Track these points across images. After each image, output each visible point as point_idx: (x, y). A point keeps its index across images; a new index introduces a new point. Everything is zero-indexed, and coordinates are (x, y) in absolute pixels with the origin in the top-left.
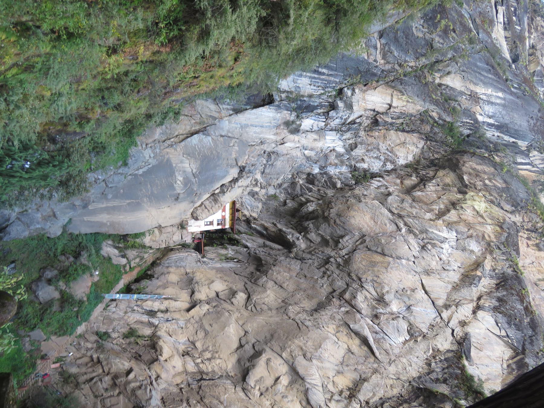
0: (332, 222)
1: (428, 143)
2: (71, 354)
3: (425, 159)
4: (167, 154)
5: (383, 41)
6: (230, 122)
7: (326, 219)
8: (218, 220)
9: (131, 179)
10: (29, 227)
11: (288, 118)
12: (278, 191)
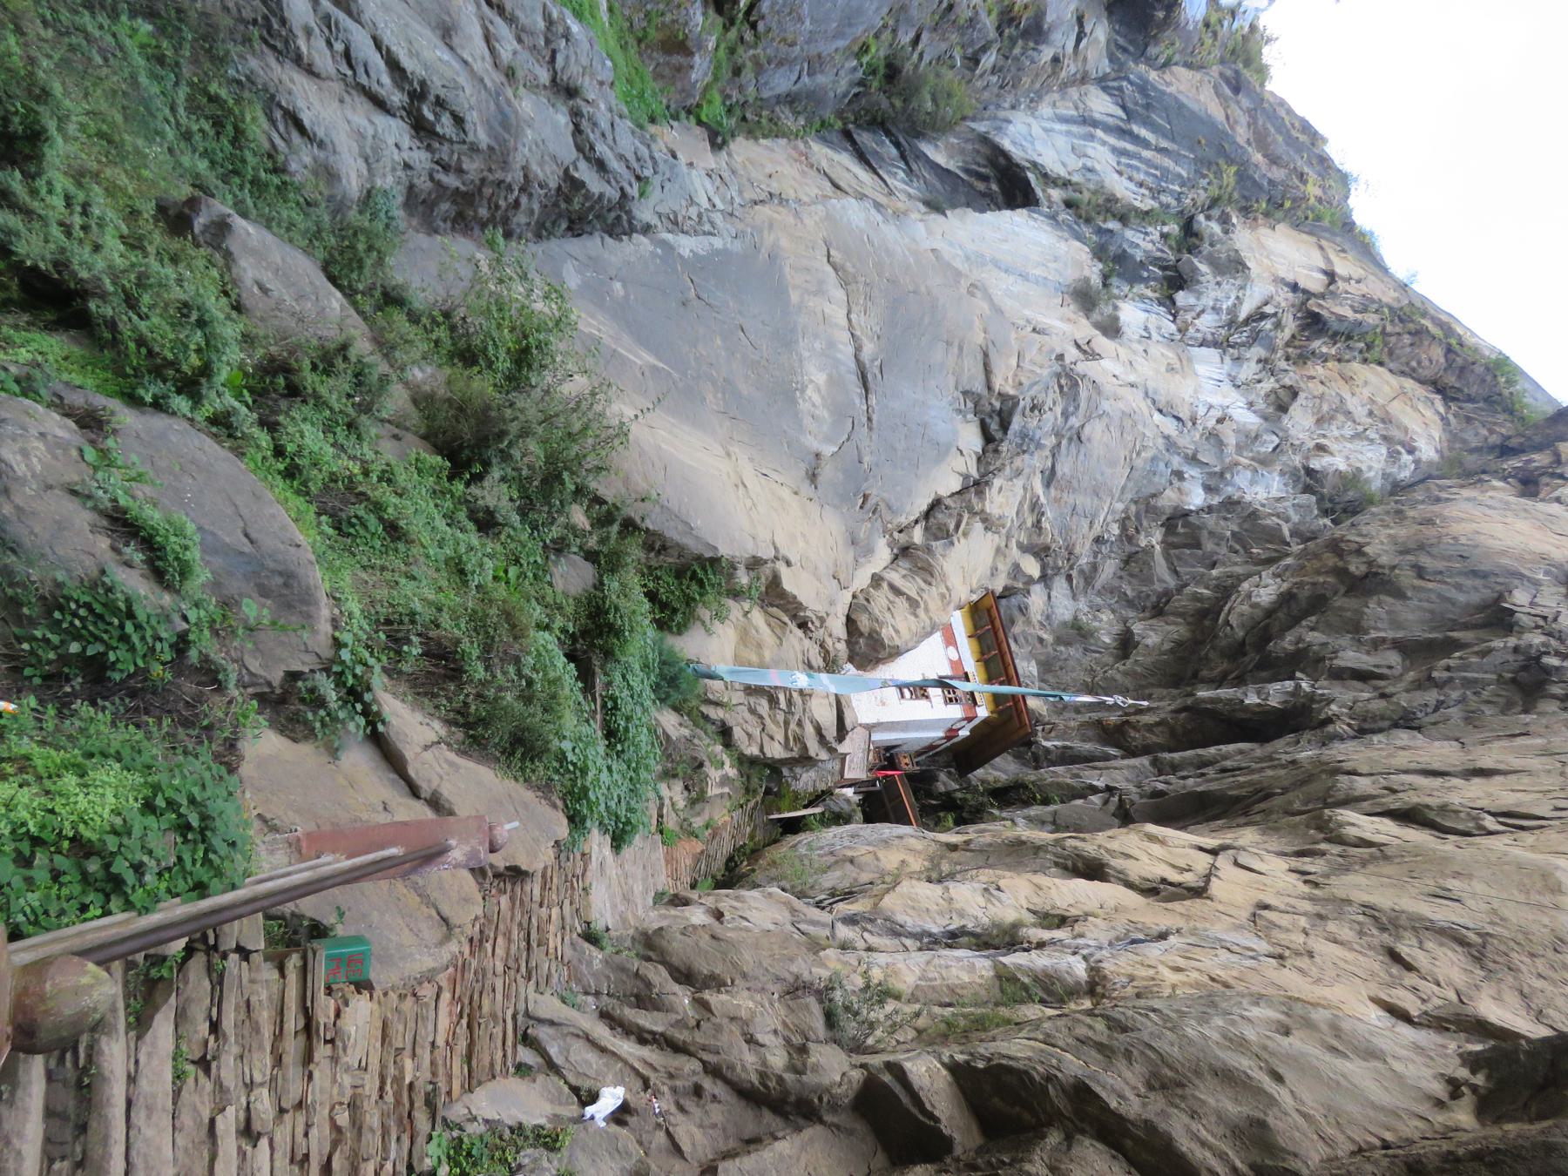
0: (1406, 578)
2: (611, 1098)
3: (1472, 451)
4: (771, 226)
7: (1372, 582)
11: (1087, 273)
12: (1083, 605)
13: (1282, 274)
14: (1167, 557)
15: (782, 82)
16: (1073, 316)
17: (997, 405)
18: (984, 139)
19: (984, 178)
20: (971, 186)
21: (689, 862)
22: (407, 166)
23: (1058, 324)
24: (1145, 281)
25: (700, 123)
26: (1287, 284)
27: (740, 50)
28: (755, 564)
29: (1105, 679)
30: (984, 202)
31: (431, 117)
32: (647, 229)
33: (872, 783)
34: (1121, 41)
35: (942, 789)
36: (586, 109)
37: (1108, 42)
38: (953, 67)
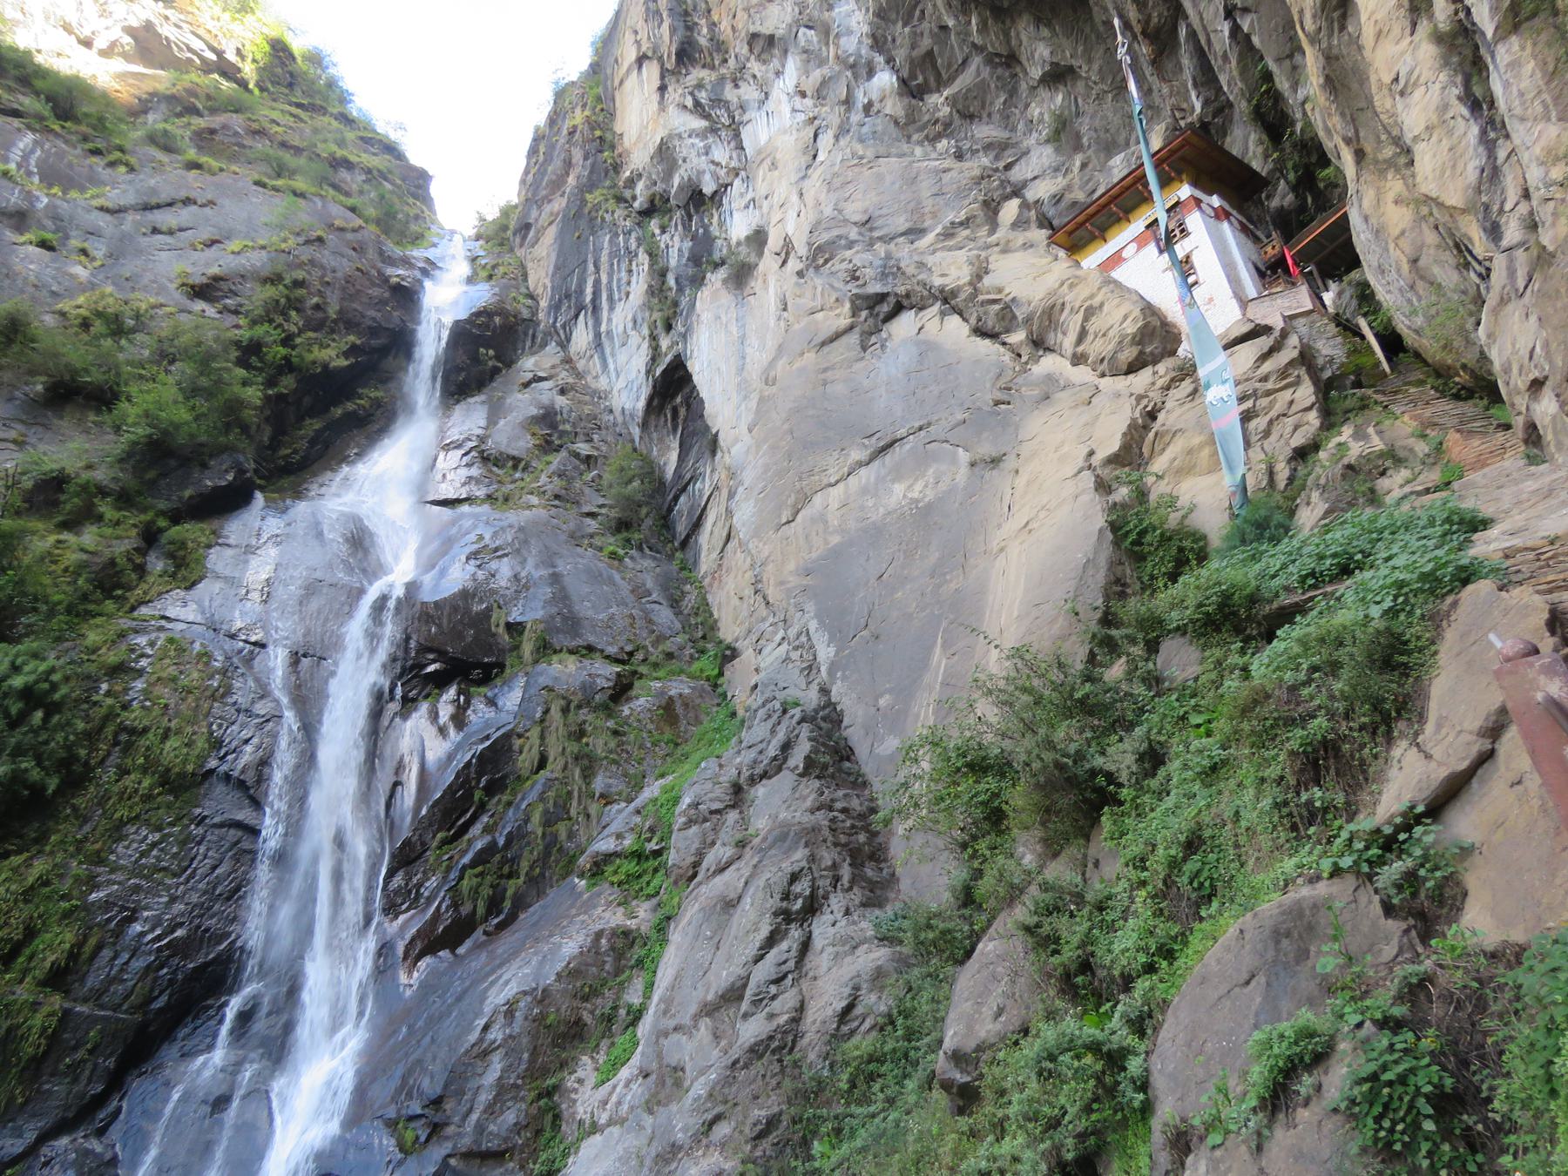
4: (782, 583)
9: (844, 678)
10: (675, 1148)
11: (719, 284)
12: (1031, 141)
13: (655, 106)
14: (952, 79)
15: (664, 615)
16: (760, 281)
17: (864, 314)
18: (644, 425)
20: (685, 420)
21: (1476, 442)
22: (847, 912)
23: (771, 290)
24: (706, 228)
25: (721, 674)
26: (662, 97)
27: (653, 659)
28: (1103, 487)
29: (1103, 79)
30: (694, 404)
31: (800, 901)
32: (824, 691)
33: (1309, 277)
34: (528, 343)
35: (1290, 197)
36: (746, 773)
37: (533, 354)
38: (600, 476)
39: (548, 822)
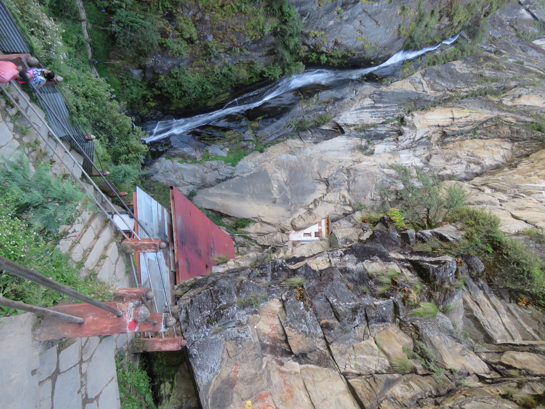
1: (516, 144)
5: (427, 78)
6: (312, 149)
8: (316, 233)
11: (359, 143)
19: (337, 129)
20: (335, 131)
24: (390, 136)
39: (218, 139)
